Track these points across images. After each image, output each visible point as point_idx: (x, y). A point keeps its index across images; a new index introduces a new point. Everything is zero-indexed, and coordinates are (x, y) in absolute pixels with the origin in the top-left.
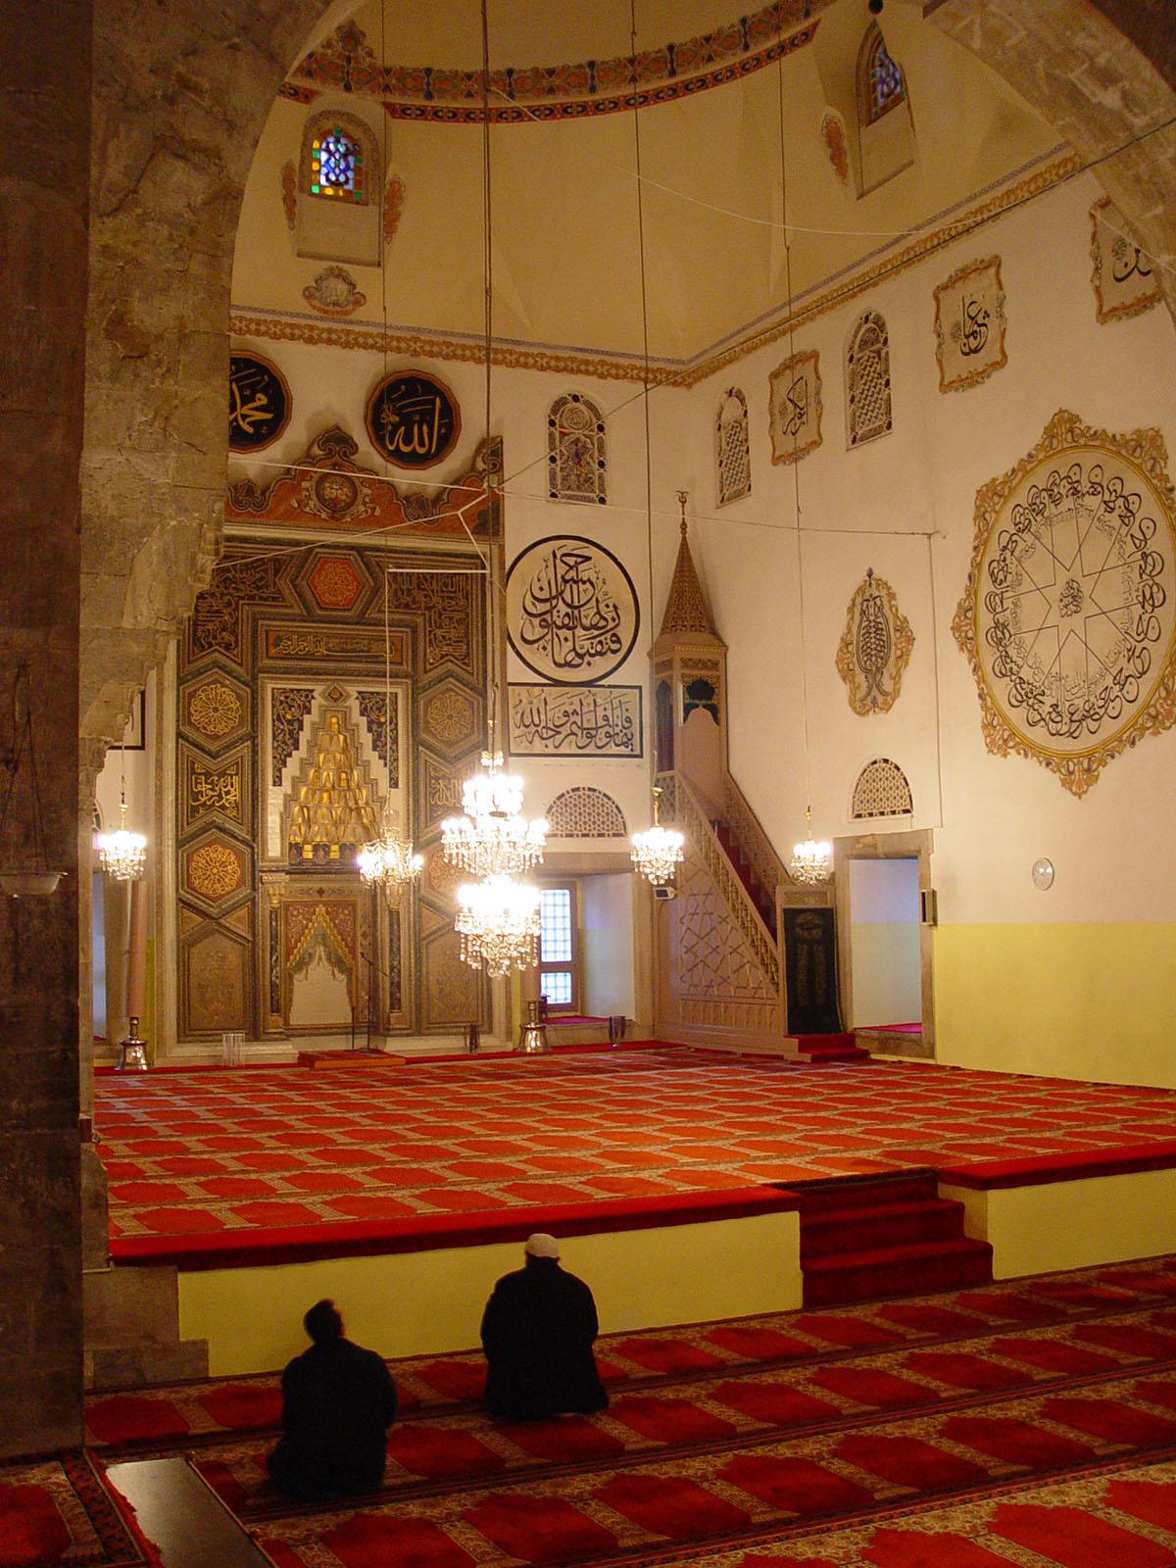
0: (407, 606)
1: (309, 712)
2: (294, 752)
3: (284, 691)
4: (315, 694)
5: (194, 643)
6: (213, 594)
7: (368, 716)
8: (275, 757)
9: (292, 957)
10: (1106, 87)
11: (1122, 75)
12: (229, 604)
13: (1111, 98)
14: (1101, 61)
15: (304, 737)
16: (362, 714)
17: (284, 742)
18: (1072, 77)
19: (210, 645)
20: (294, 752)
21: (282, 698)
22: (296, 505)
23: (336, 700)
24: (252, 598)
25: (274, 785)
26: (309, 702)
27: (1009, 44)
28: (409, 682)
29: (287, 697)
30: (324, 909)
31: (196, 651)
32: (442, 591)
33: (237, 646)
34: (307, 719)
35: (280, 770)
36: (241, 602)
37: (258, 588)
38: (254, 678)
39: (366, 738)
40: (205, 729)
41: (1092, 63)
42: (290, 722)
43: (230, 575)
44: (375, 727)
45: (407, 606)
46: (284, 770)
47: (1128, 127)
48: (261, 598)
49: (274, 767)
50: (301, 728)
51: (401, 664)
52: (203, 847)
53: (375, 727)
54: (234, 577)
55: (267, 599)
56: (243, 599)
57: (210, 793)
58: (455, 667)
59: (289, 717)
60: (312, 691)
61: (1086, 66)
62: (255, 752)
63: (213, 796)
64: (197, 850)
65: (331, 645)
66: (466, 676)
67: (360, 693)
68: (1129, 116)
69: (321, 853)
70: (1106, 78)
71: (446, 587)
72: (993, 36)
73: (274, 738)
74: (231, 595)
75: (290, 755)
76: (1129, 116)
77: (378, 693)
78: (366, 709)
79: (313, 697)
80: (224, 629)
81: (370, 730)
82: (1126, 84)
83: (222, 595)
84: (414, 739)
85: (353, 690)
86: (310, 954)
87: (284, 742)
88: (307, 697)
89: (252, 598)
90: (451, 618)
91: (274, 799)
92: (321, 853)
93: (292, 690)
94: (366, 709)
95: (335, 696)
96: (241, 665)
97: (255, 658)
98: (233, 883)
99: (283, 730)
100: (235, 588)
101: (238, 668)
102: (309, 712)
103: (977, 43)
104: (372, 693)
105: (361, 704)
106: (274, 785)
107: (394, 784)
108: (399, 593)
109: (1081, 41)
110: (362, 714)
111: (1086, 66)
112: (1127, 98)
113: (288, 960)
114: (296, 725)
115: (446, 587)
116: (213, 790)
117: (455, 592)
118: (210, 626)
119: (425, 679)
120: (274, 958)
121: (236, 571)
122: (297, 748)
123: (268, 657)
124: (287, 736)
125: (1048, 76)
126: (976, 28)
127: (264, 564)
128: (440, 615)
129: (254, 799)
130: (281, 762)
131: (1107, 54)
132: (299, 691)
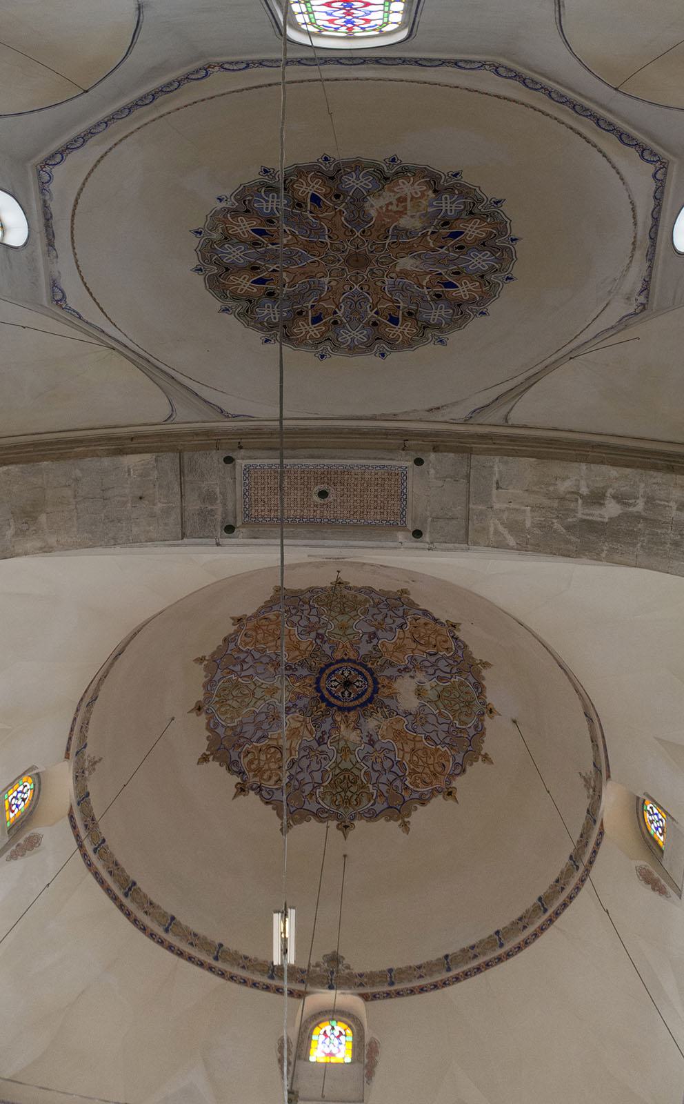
10: (602, 504)
11: (603, 488)
13: (612, 509)
14: (584, 490)
18: (580, 515)
27: (528, 524)
41: (582, 496)
47: (638, 517)
61: (580, 501)
68: (631, 509)
70: (596, 499)
72: (515, 527)
76: (631, 509)
82: (610, 491)
103: (511, 541)
109: (564, 487)
111: (580, 501)
112: (620, 499)
125: (568, 528)
126: (501, 528)
131: (583, 483)
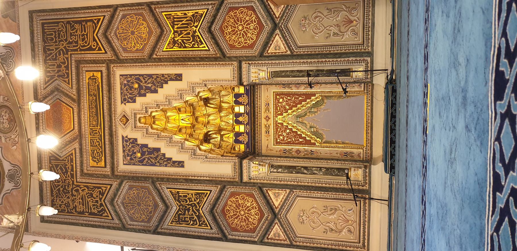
0: (67, 67)
1: (136, 140)
2: (162, 151)
3: (124, 156)
4: (125, 136)
5: (101, 215)
6: (73, 201)
7: (136, 96)
8: (166, 166)
9: (312, 141)
12: (77, 191)
15: (152, 144)
16: (134, 101)
17: (156, 158)
19: (101, 205)
20: (162, 151)
21: (129, 158)
22: (15, 147)
23: (128, 120)
24: (72, 175)
25: (183, 166)
26: (130, 139)
28: (112, 66)
29: (128, 155)
30: (279, 117)
31: (106, 214)
32: (56, 42)
33: (100, 188)
34: (140, 141)
35: (174, 162)
36: (75, 183)
37: (67, 172)
38: (117, 177)
39: (150, 97)
40: (151, 212)
42: (143, 154)
43: (61, 189)
44: (143, 92)
45: (67, 67)
46: (173, 160)
48: (72, 170)
49: (172, 166)
50: (146, 146)
51: (101, 71)
52: (226, 220)
53: (143, 92)
54: (61, 187)
55: (72, 166)
56: (73, 181)
57: (191, 212)
58: (101, 31)
59: (139, 155)
60: (123, 136)
62: (162, 179)
63: (193, 211)
64: (228, 224)
65: (94, 123)
66: (106, 21)
67: (122, 103)
69: (240, 119)
71: (52, 39)
73: (153, 165)
74: (72, 189)
75: (164, 155)
77: (121, 89)
78: (131, 98)
79: (127, 137)
80: (92, 195)
81: (145, 95)
83: (73, 195)
84: (148, 62)
85: (120, 108)
86: (311, 127)
87: (156, 158)
88: (127, 141)
89: (72, 175)
90: (71, 35)
91: (195, 167)
92: (240, 119)
93: (124, 151)
94: (131, 98)
95: (125, 119)
96: (111, 185)
97: (105, 176)
98: (250, 199)
99: (148, 159)
100: (68, 187)
101: (113, 187)
102: (136, 140)
104: (121, 93)
105: (128, 102)
106: (183, 166)
107: (178, 77)
108: (60, 73)
110: (134, 101)
113: (314, 144)
114: (145, 149)
115: (52, 39)
116: (189, 210)
117: (55, 32)
118: (91, 204)
119: (110, 55)
120: (305, 171)
121: (59, 185)
122: (158, 150)
123: (105, 167)
124: (152, 156)
127: (53, 166)
128: (70, 43)
129: (192, 181)
130: (169, 162)
132: (123, 147)
